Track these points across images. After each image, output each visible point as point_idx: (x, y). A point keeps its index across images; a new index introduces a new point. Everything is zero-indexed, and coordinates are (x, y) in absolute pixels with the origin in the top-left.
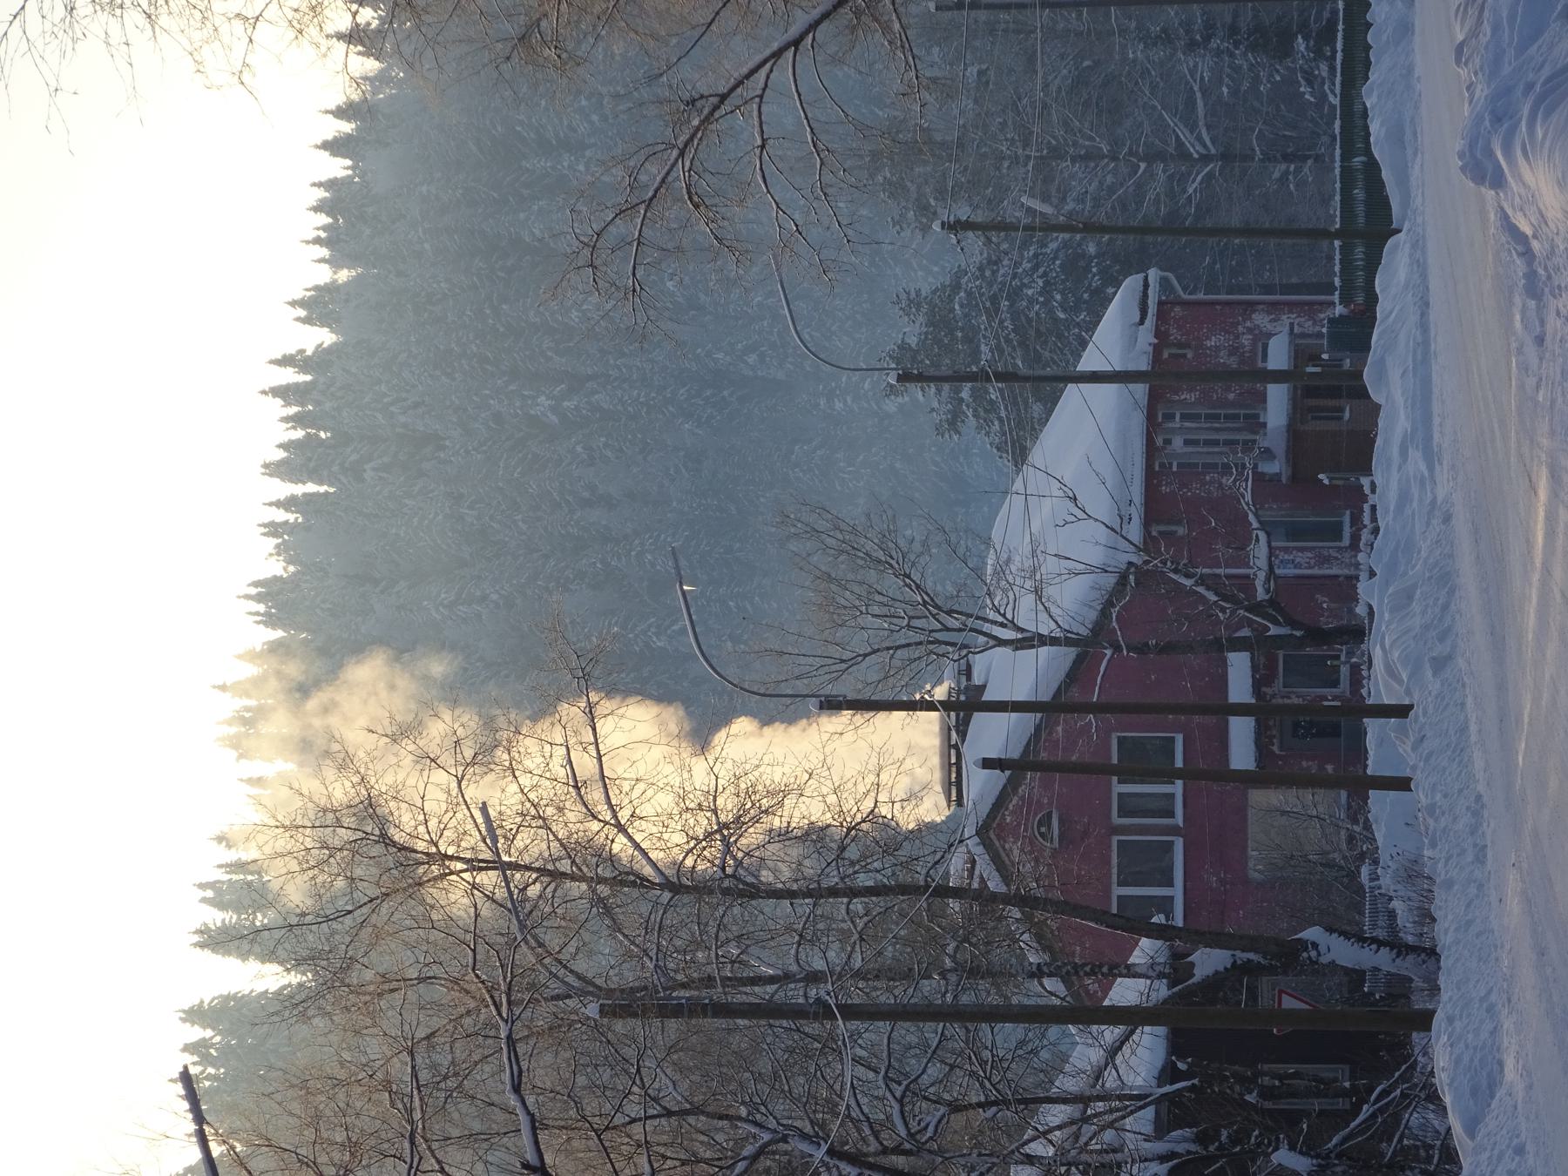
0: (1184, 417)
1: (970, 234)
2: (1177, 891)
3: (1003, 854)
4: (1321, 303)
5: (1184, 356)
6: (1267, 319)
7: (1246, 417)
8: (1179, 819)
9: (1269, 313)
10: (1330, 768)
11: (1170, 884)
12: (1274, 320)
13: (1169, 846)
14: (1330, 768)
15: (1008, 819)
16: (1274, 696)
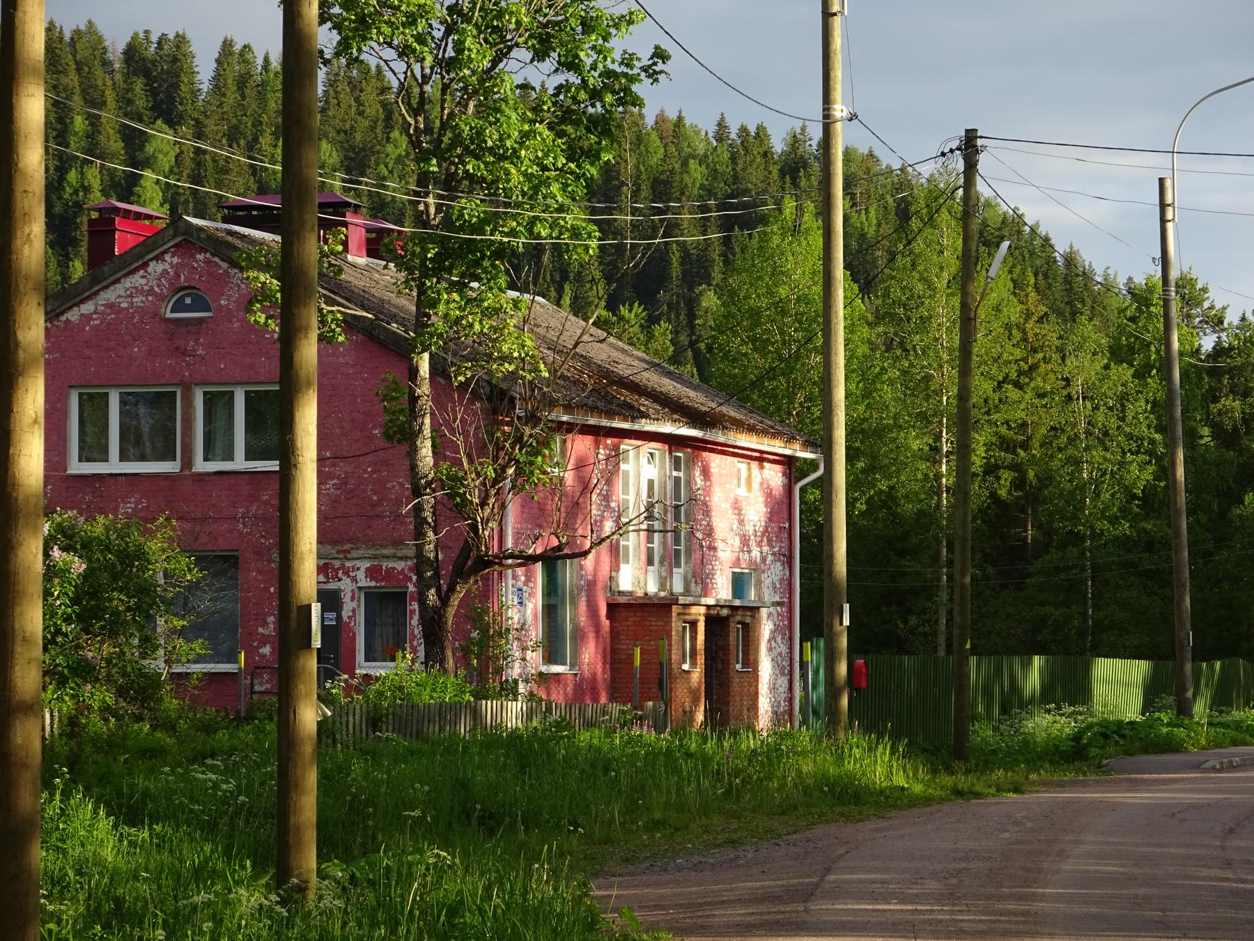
0: (677, 480)
1: (960, 165)
2: (114, 465)
3: (157, 252)
4: (791, 639)
5: (739, 485)
6: (776, 579)
7: (677, 552)
8: (201, 466)
9: (781, 580)
10: (266, 650)
11: (124, 457)
12: (774, 588)
13: (168, 455)
14: (266, 650)
15: (200, 257)
16: (354, 580)
